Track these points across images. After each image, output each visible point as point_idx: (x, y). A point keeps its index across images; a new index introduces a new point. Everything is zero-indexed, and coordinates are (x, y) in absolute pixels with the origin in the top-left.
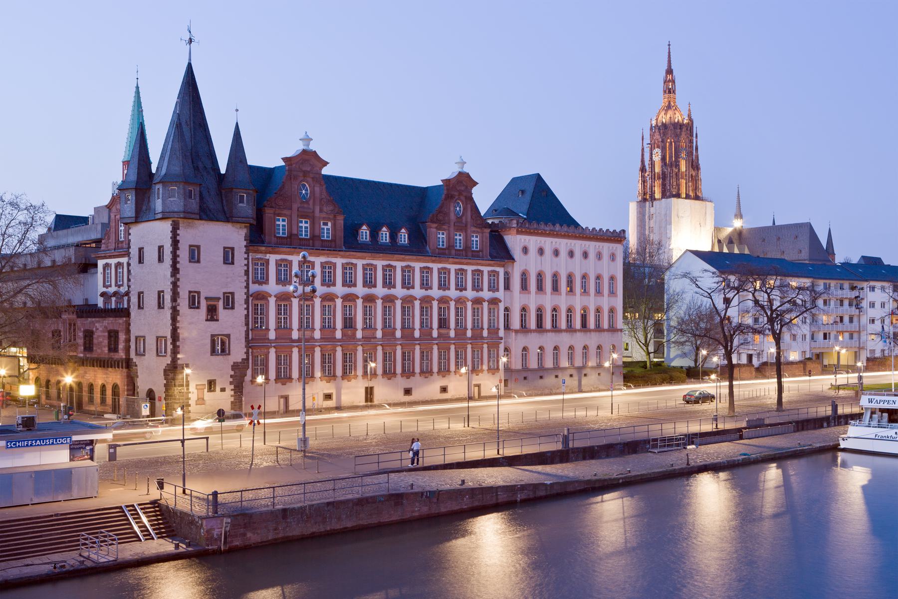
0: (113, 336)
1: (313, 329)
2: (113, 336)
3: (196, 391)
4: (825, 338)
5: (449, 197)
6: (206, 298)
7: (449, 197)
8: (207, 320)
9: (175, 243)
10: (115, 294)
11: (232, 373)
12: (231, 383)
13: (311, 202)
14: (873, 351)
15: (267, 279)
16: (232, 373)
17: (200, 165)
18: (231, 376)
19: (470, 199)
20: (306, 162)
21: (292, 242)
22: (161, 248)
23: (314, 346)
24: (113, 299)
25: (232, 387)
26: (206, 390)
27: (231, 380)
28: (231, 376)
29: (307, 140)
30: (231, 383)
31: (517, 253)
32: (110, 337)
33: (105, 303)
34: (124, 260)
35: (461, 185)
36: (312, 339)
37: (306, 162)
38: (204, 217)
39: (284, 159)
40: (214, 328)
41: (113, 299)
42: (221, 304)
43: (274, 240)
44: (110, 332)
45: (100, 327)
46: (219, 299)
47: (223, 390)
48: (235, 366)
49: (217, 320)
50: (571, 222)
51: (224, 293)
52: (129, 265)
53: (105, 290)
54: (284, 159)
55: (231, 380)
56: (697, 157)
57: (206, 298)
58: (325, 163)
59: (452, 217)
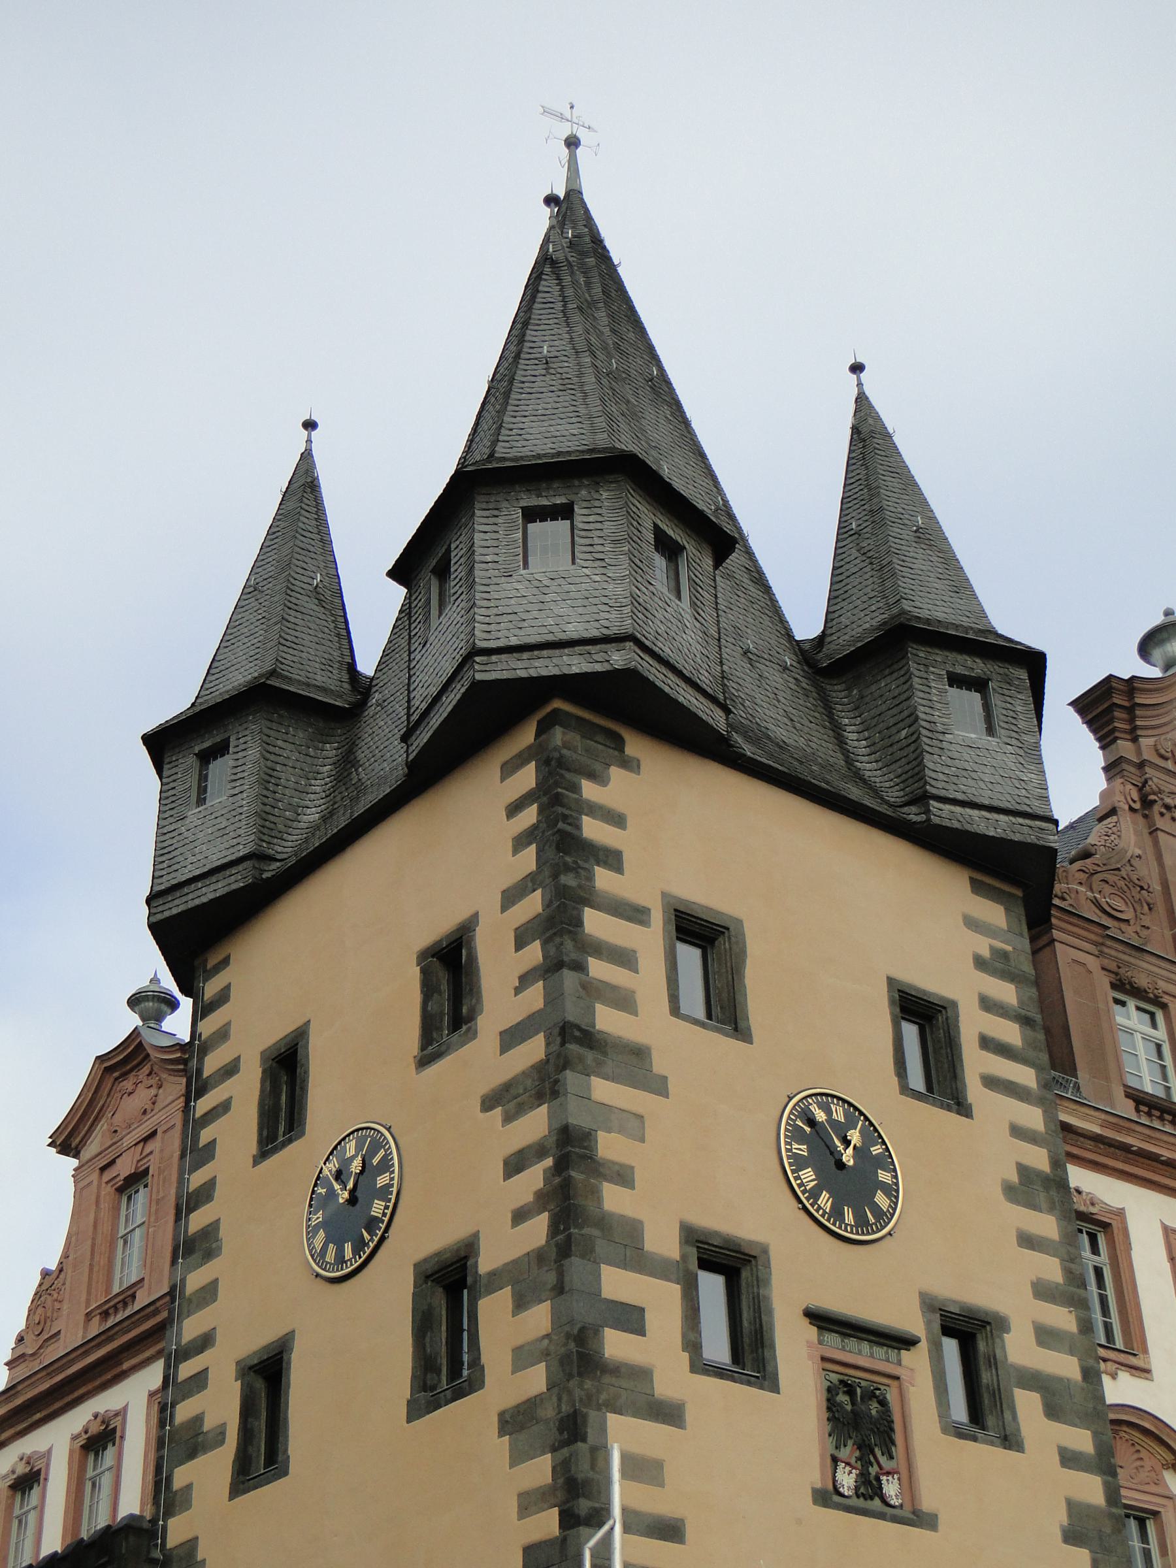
6: (821, 1320)
8: (828, 1497)
9: (564, 854)
46: (907, 1342)
49: (921, 1519)
57: (821, 1320)
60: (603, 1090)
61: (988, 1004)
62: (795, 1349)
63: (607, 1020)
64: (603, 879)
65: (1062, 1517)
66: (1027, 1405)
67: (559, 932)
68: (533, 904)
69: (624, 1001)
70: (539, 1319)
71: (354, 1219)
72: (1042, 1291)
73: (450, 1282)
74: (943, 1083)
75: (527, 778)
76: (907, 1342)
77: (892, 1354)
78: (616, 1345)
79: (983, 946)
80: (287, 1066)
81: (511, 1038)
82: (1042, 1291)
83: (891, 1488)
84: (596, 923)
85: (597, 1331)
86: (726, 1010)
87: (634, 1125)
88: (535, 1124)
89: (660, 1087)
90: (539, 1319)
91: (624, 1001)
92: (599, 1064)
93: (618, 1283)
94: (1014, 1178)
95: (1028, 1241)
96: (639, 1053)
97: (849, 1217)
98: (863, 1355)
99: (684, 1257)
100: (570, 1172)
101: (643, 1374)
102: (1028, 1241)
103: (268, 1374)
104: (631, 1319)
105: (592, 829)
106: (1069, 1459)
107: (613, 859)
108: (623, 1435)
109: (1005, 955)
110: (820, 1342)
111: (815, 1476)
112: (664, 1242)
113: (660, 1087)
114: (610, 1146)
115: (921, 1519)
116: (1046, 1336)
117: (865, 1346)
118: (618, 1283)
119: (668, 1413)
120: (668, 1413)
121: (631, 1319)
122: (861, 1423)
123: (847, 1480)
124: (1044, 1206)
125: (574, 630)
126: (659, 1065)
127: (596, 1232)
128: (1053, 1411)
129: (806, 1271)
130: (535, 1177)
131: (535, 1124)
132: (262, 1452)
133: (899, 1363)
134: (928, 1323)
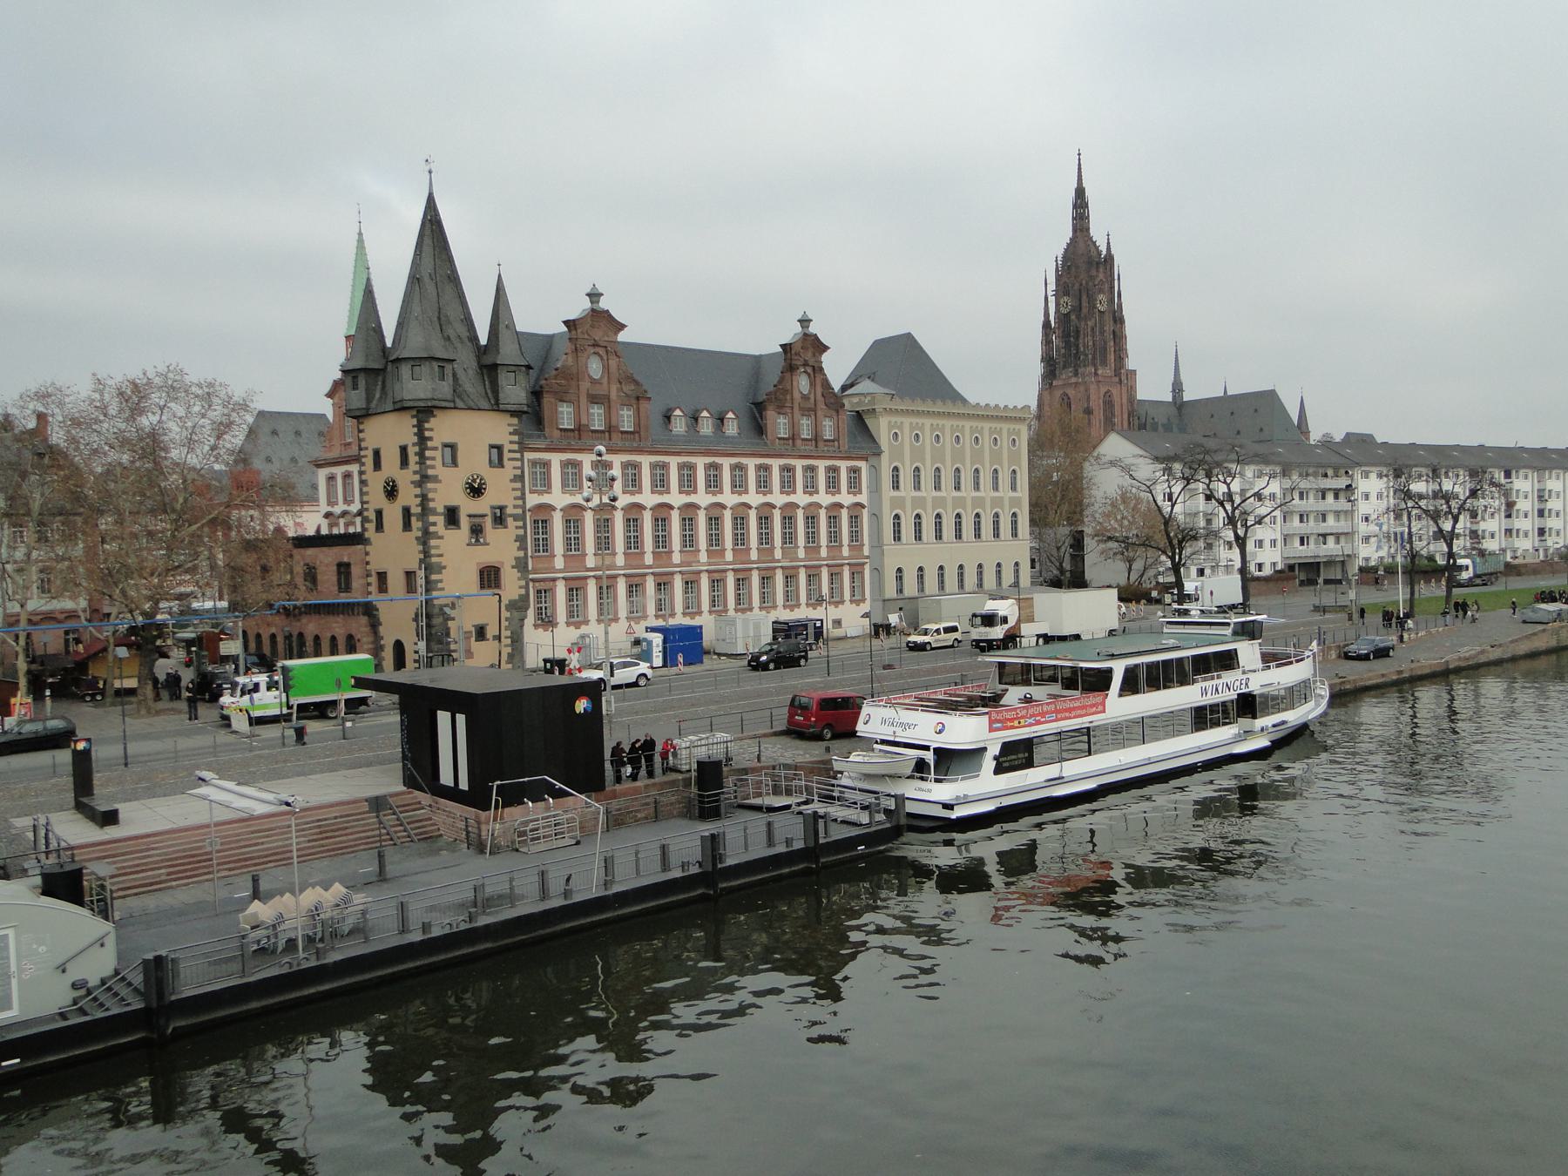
0: (344, 569)
1: (614, 554)
2: (344, 569)
4: (1302, 543)
5: (791, 368)
7: (791, 368)
9: (422, 440)
10: (344, 514)
13: (605, 381)
14: (1367, 559)
15: (550, 487)
17: (451, 332)
19: (818, 370)
20: (595, 326)
21: (579, 436)
22: (404, 449)
23: (615, 577)
24: (342, 521)
29: (594, 296)
31: (884, 440)
32: (339, 573)
33: (331, 526)
34: (354, 468)
35: (805, 351)
36: (613, 567)
37: (595, 326)
38: (460, 404)
39: (566, 323)
41: (342, 521)
42: (488, 521)
43: (557, 433)
44: (340, 565)
45: (326, 559)
46: (483, 516)
48: (512, 606)
50: (957, 397)
51: (493, 508)
52: (361, 473)
53: (330, 509)
54: (566, 323)
56: (1120, 306)
58: (622, 327)
59: (797, 395)
60: (429, 485)
62: (465, 523)
63: (430, 472)
64: (429, 444)
66: (510, 520)
67: (421, 454)
68: (417, 449)
69: (433, 467)
70: (420, 524)
71: (391, 492)
73: (407, 512)
74: (501, 464)
75: (415, 421)
78: (432, 529)
79: (511, 429)
80: (377, 453)
81: (415, 473)
84: (428, 453)
86: (455, 463)
87: (435, 490)
88: (418, 491)
90: (420, 524)
91: (433, 467)
93: (432, 519)
98: (477, 520)
100: (424, 499)
103: (379, 513)
104: (434, 524)
105: (427, 434)
107: (430, 439)
108: (433, 542)
112: (441, 509)
114: (430, 496)
116: (515, 507)
118: (432, 519)
121: (434, 524)
122: (477, 531)
125: (422, 396)
129: (467, 506)
130: (418, 500)
131: (418, 491)
132: (380, 527)
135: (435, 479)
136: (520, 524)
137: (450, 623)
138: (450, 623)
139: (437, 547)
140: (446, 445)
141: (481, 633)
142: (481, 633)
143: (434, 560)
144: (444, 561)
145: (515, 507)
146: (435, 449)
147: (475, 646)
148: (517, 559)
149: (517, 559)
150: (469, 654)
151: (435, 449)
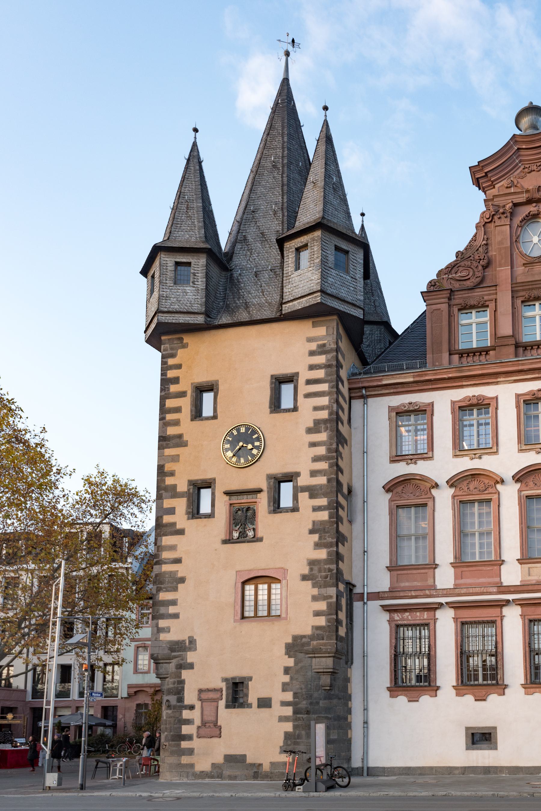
3: (198, 705)
11: (291, 662)
12: (285, 687)
16: (291, 662)
18: (287, 670)
25: (289, 696)
26: (222, 703)
27: (287, 679)
28: (287, 670)
30: (285, 687)
40: (249, 558)
42: (262, 503)
46: (260, 491)
47: (265, 703)
49: (256, 539)
55: (287, 679)
61: (312, 367)
65: (310, 526)
69: (177, 423)
72: (316, 459)
76: (260, 491)
77: (254, 496)
82: (316, 459)
83: (251, 534)
85: (162, 517)
89: (185, 444)
92: (167, 444)
94: (311, 425)
95: (313, 445)
96: (180, 436)
97: (242, 460)
98: (244, 500)
99: (189, 490)
101: (174, 524)
102: (313, 445)
106: (316, 509)
109: (324, 345)
110: (230, 500)
111: (223, 536)
112: (183, 487)
113: (185, 444)
115: (261, 540)
116: (314, 473)
117: (245, 496)
119: (181, 532)
120: (181, 532)
121: (172, 511)
123: (236, 535)
124: (323, 430)
126: (185, 438)
127: (163, 492)
128: (312, 497)
133: (256, 498)
134: (269, 484)
135: (179, 441)
136: (323, 501)
137: (185, 674)
138: (185, 674)
139: (173, 548)
140: (200, 390)
141: (237, 692)
142: (237, 692)
143: (165, 568)
144: (180, 570)
145: (314, 473)
146: (182, 394)
147: (227, 716)
148: (312, 563)
149: (312, 563)
150: (212, 728)
151: (182, 394)
